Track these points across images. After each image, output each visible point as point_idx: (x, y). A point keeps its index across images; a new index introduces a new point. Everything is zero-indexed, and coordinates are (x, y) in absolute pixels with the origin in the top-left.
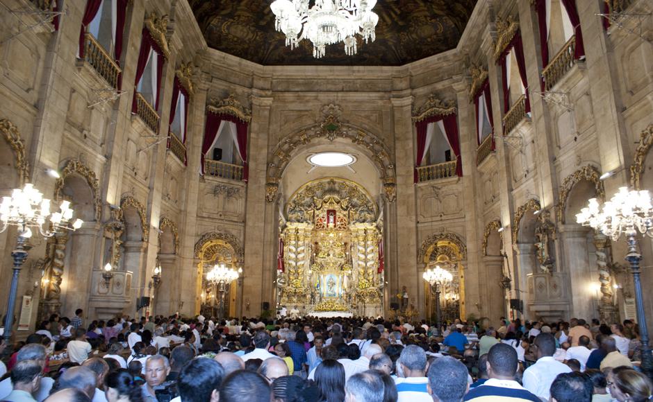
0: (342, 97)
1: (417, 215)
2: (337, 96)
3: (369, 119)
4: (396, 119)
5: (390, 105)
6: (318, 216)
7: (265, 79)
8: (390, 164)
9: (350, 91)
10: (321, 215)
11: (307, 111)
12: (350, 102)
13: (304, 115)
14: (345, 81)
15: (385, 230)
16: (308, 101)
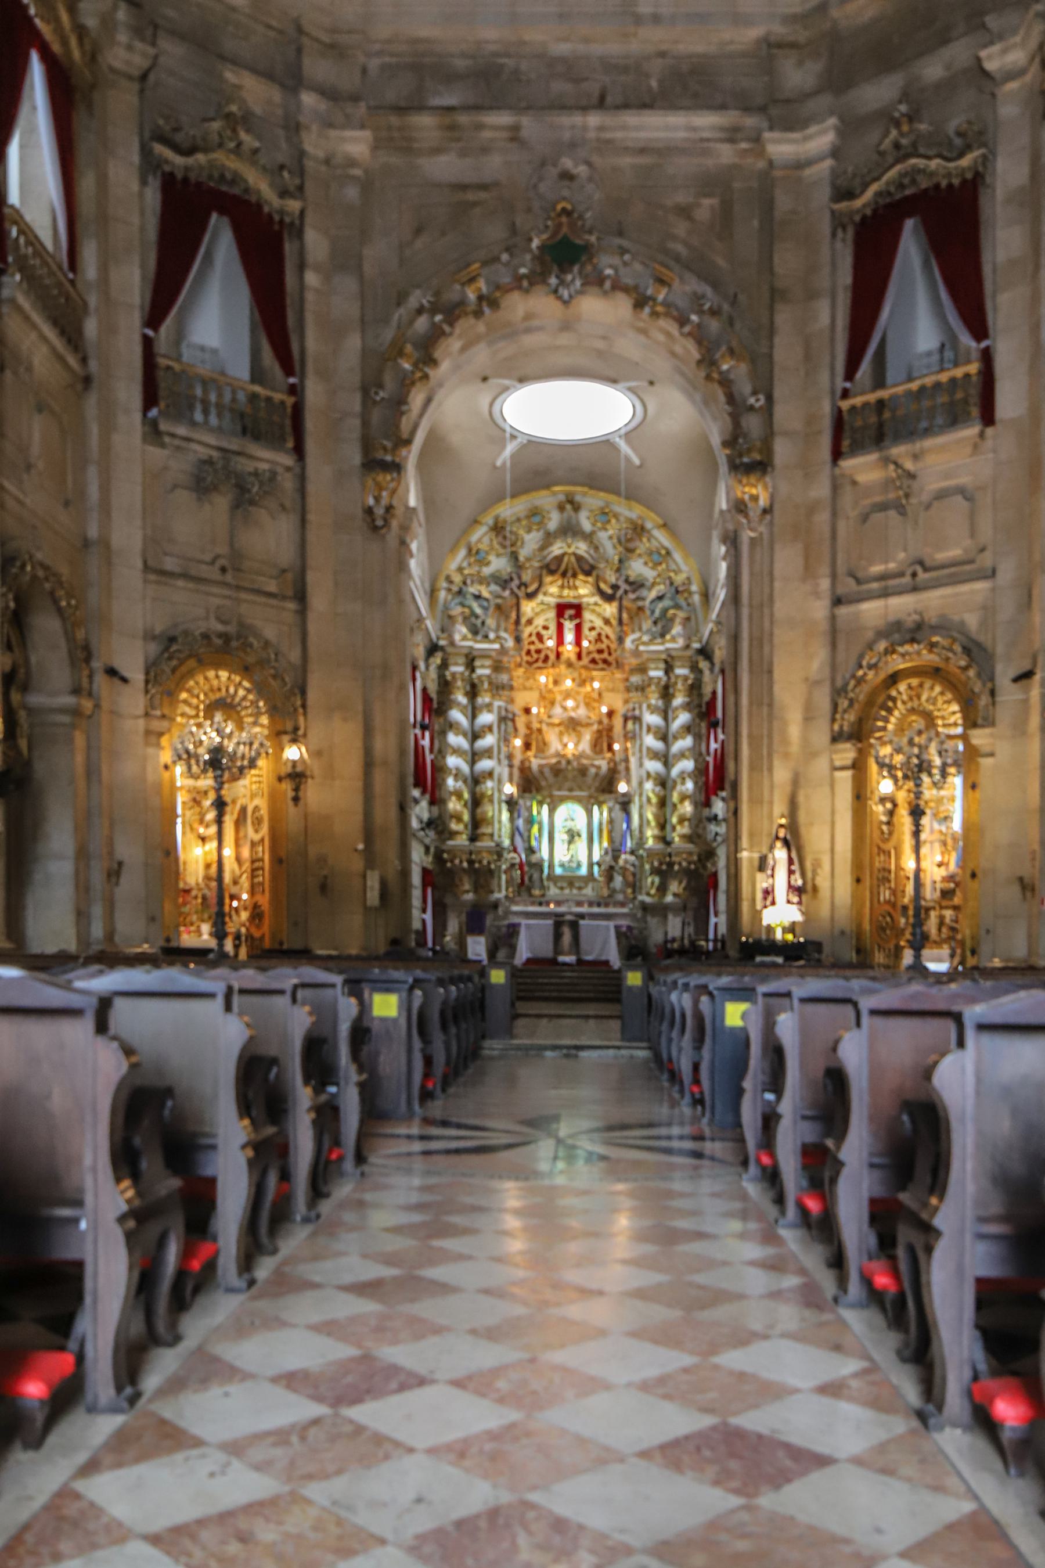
0: (601, 128)
1: (834, 576)
2: (585, 128)
3: (689, 218)
4: (778, 214)
5: (761, 164)
6: (530, 622)
7: (335, 50)
8: (755, 393)
9: (626, 106)
10: (539, 622)
11: (484, 187)
12: (627, 150)
13: (475, 204)
14: (609, 66)
15: (735, 639)
16: (485, 150)
